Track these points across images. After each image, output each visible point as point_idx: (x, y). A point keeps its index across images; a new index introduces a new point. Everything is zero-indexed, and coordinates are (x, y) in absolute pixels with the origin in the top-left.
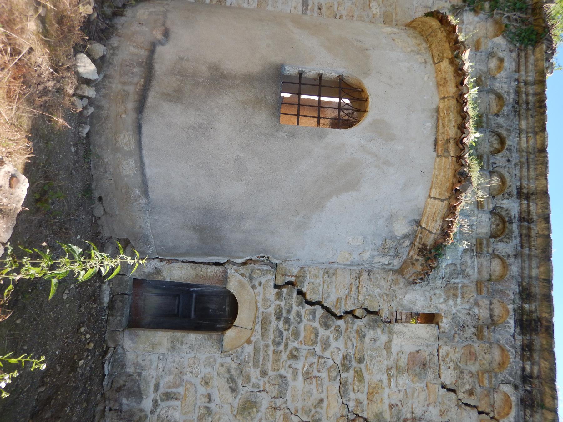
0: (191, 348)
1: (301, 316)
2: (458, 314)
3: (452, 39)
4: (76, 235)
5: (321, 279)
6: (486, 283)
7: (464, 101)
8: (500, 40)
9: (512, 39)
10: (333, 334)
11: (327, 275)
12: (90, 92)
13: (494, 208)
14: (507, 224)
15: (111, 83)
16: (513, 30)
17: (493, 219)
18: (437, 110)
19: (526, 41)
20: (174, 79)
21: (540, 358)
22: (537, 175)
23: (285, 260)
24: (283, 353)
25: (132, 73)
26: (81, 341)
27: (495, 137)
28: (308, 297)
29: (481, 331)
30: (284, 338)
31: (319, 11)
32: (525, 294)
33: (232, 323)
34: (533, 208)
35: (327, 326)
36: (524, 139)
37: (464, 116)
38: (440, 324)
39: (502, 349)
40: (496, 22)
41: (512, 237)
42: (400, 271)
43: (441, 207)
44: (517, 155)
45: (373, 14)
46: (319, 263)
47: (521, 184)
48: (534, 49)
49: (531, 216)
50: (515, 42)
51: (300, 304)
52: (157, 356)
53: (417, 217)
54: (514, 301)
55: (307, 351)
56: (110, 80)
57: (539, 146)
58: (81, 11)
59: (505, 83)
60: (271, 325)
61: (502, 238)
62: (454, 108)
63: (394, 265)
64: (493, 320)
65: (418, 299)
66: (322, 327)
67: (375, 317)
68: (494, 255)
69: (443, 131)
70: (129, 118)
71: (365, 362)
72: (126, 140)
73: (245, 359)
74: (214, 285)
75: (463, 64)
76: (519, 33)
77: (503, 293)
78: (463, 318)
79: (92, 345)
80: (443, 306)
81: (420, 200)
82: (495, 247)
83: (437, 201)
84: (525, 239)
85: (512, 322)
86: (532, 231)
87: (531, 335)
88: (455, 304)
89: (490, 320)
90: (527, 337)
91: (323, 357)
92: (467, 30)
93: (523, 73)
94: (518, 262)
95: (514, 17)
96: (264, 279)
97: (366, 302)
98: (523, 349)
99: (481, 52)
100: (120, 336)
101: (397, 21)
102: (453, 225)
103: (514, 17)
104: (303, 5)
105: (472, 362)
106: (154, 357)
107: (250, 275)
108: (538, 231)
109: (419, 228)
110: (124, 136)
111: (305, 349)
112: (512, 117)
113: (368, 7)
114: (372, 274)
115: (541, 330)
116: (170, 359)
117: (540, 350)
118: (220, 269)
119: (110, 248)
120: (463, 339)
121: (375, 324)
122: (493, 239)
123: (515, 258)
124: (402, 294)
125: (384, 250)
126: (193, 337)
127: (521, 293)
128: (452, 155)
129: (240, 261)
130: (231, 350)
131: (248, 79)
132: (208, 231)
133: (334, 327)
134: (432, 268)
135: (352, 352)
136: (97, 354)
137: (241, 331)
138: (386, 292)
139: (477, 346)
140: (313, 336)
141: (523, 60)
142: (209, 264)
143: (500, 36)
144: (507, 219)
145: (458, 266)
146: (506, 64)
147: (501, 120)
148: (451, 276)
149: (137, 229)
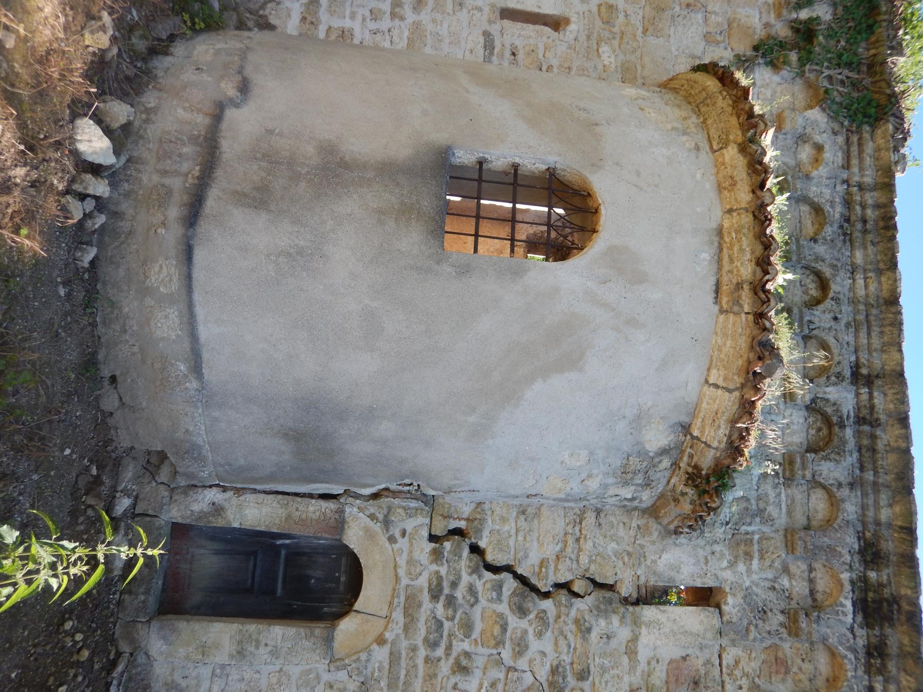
0: (275, 653)
1: (477, 593)
2: (754, 588)
3: (742, 109)
4: (63, 450)
5: (513, 525)
6: (802, 534)
7: (766, 217)
8: (816, 115)
9: (837, 113)
10: (534, 626)
11: (522, 518)
12: (100, 187)
13: (813, 401)
14: (836, 428)
15: (140, 171)
16: (837, 99)
17: (811, 420)
18: (720, 232)
19: (860, 116)
20: (256, 167)
21: (899, 669)
22: (884, 345)
23: (449, 491)
24: (442, 662)
25: (180, 155)
26: (63, 647)
27: (811, 277)
28: (489, 558)
29: (796, 621)
30: (445, 634)
31: (513, 57)
32: (870, 553)
33: (352, 605)
34: (878, 400)
35: (522, 612)
37: (767, 244)
38: (723, 607)
39: (833, 654)
40: (809, 85)
41: (844, 451)
42: (653, 512)
43: (728, 402)
44: (850, 309)
45: (604, 66)
46: (508, 497)
47: (857, 358)
48: (873, 131)
49: (876, 416)
50: (842, 119)
51: (474, 571)
52: (209, 669)
53: (685, 419)
54: (851, 566)
55: (486, 658)
56: (139, 166)
57: (885, 294)
58: (87, 43)
60: (423, 609)
61: (829, 454)
62: (749, 229)
63: (641, 501)
64: (814, 600)
65: (681, 561)
66: (514, 614)
67: (608, 594)
68: (815, 483)
69: (730, 268)
70: (171, 235)
71: (591, 678)
72: (164, 274)
73: (373, 674)
74: (319, 535)
75: (764, 153)
76: (847, 104)
77: (831, 551)
78: (764, 596)
79: (86, 654)
80: (728, 575)
81: (689, 388)
82: (816, 468)
83: (720, 391)
84: (867, 455)
85: (849, 604)
86: (879, 441)
87: (882, 628)
88: (749, 571)
89: (809, 600)
90: (875, 632)
91: (516, 670)
93: (855, 170)
94: (856, 496)
96: (410, 525)
97: (593, 567)
98: (869, 654)
99: (785, 134)
100: (142, 630)
101: (644, 78)
102: (749, 434)
103: (840, 77)
104: (485, 47)
105: (780, 676)
106: (205, 672)
107: (386, 516)
108: (888, 441)
109: (689, 437)
110: (161, 267)
111: (483, 653)
112: (839, 244)
113: (596, 53)
114: (602, 515)
115: (899, 619)
116: (234, 675)
117: (899, 656)
118: (331, 505)
119: (131, 468)
120: (764, 635)
121: (610, 608)
122: (813, 455)
123: (851, 489)
124: (655, 553)
125: (625, 475)
126: (278, 633)
127: (862, 552)
128: (746, 310)
129: (367, 491)
130: (348, 656)
131: (388, 170)
132: (310, 441)
133: (536, 612)
134: (710, 510)
135: (568, 660)
136: (96, 667)
137: (367, 621)
138: (627, 548)
139: (788, 647)
140: (497, 630)
141: (854, 149)
142: (311, 496)
143: (817, 108)
144: (835, 419)
145: (753, 502)
146: (827, 155)
147: (820, 249)
148: (741, 521)
149: (179, 435)
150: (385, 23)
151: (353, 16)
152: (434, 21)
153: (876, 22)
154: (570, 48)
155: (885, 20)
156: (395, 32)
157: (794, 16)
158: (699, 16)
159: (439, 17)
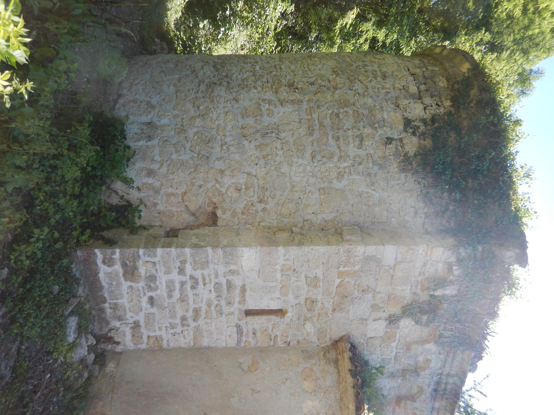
8: (431, 346)
31: (254, 335)
45: (308, 333)
48: (464, 351)
59: (428, 378)
92: (401, 333)
104: (238, 333)
146: (432, 365)
150: (179, 329)
151: (160, 329)
152: (206, 323)
155: (490, 299)
156: (186, 333)
158: (370, 296)
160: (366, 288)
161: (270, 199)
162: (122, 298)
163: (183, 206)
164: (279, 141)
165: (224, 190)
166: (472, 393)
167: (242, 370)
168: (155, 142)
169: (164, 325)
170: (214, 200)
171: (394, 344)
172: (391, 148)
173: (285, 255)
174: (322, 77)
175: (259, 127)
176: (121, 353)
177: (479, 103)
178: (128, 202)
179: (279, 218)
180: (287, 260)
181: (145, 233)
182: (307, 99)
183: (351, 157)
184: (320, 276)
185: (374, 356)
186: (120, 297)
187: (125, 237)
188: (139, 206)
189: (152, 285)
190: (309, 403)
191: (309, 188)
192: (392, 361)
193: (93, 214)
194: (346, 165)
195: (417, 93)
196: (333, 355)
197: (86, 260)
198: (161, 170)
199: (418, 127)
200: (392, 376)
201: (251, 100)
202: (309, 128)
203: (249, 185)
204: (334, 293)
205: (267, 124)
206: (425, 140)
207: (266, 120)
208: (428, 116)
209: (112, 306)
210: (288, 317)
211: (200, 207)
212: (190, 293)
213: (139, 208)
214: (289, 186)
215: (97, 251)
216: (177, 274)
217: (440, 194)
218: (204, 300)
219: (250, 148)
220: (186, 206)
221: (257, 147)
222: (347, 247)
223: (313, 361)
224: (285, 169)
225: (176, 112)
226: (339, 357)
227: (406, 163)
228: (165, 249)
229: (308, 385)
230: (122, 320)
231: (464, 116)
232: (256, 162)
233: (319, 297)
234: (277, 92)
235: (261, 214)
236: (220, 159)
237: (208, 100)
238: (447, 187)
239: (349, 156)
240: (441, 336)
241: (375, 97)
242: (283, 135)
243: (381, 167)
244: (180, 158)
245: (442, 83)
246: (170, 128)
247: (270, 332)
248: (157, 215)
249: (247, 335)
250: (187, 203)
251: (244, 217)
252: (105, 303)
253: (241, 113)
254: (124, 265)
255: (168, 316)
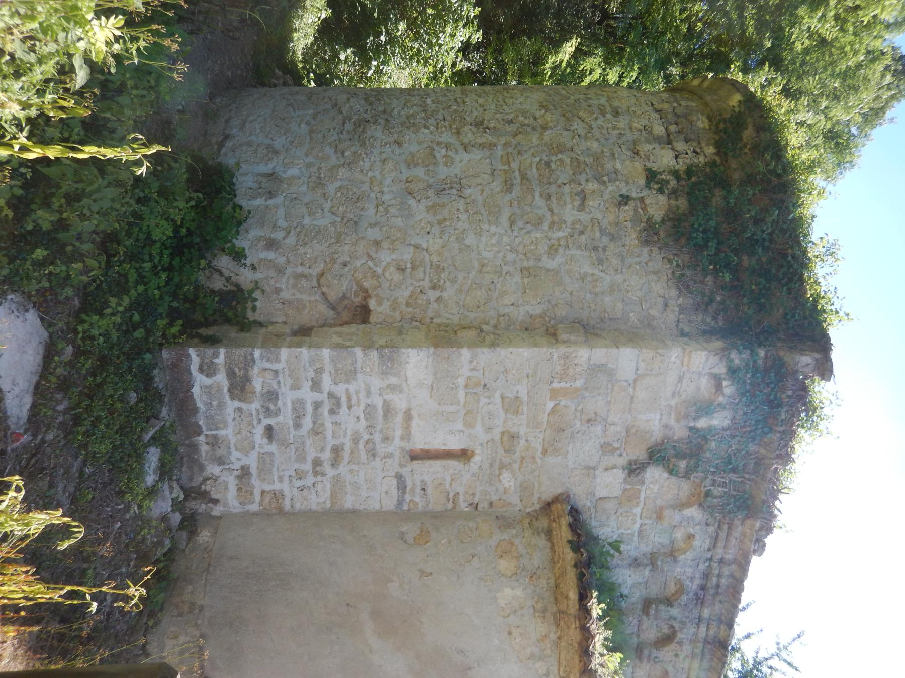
8: (693, 512)
31: (423, 492)
36: (703, 629)
45: (505, 489)
59: (690, 566)
95: (723, 480)
103: (723, 480)
143: (696, 506)
146: (697, 543)
147: (675, 611)
150: (309, 480)
152: (351, 471)
153: (771, 430)
154: (473, 475)
155: (780, 432)
156: (319, 487)
157: (692, 425)
158: (599, 429)
159: (355, 467)
160: (592, 416)
161: (448, 284)
162: (226, 426)
163: (319, 292)
164: (462, 200)
165: (379, 270)
166: (774, 662)
167: (405, 542)
168: (279, 200)
169: (287, 473)
170: (366, 284)
171: (637, 511)
172: (628, 211)
173: (471, 362)
174: (524, 113)
175: (431, 181)
176: (220, 518)
177: (755, 147)
178: (237, 285)
179: (461, 311)
180: (473, 369)
181: (263, 331)
182: (503, 140)
183: (569, 224)
184: (524, 395)
185: (606, 528)
186: (222, 426)
187: (233, 335)
188: (252, 291)
189: (272, 407)
190: (508, 591)
191: (506, 268)
192: (635, 539)
193: (186, 300)
194: (560, 234)
195: (665, 135)
196: (543, 523)
197: (175, 365)
198: (287, 241)
199: (667, 182)
200: (635, 563)
201: (420, 143)
202: (506, 182)
203: (418, 263)
204: (545, 424)
205: (444, 177)
206: (677, 200)
207: (443, 172)
208: (681, 166)
209: (210, 440)
210: (474, 463)
211: (344, 297)
212: (327, 420)
213: (254, 295)
214: (476, 264)
215: (192, 352)
216: (309, 390)
217: (702, 278)
218: (349, 433)
219: (419, 210)
220: (323, 294)
221: (429, 209)
222: (563, 349)
223: (514, 532)
224: (470, 240)
225: (310, 159)
226: (554, 525)
227: (650, 233)
228: (293, 349)
229: (505, 565)
230: (224, 464)
231: (734, 166)
232: (428, 230)
233: (523, 431)
234: (458, 133)
235: (435, 305)
236: (375, 225)
237: (357, 143)
238: (711, 267)
239: (565, 222)
240: (708, 494)
241: (602, 139)
242: (467, 192)
243: (613, 238)
244: (315, 223)
245: (702, 123)
246: (301, 181)
247: (448, 486)
248: (280, 306)
249: (413, 490)
250: (324, 289)
251: (410, 310)
252: (199, 435)
253: (405, 161)
254: (231, 374)
255: (294, 457)
